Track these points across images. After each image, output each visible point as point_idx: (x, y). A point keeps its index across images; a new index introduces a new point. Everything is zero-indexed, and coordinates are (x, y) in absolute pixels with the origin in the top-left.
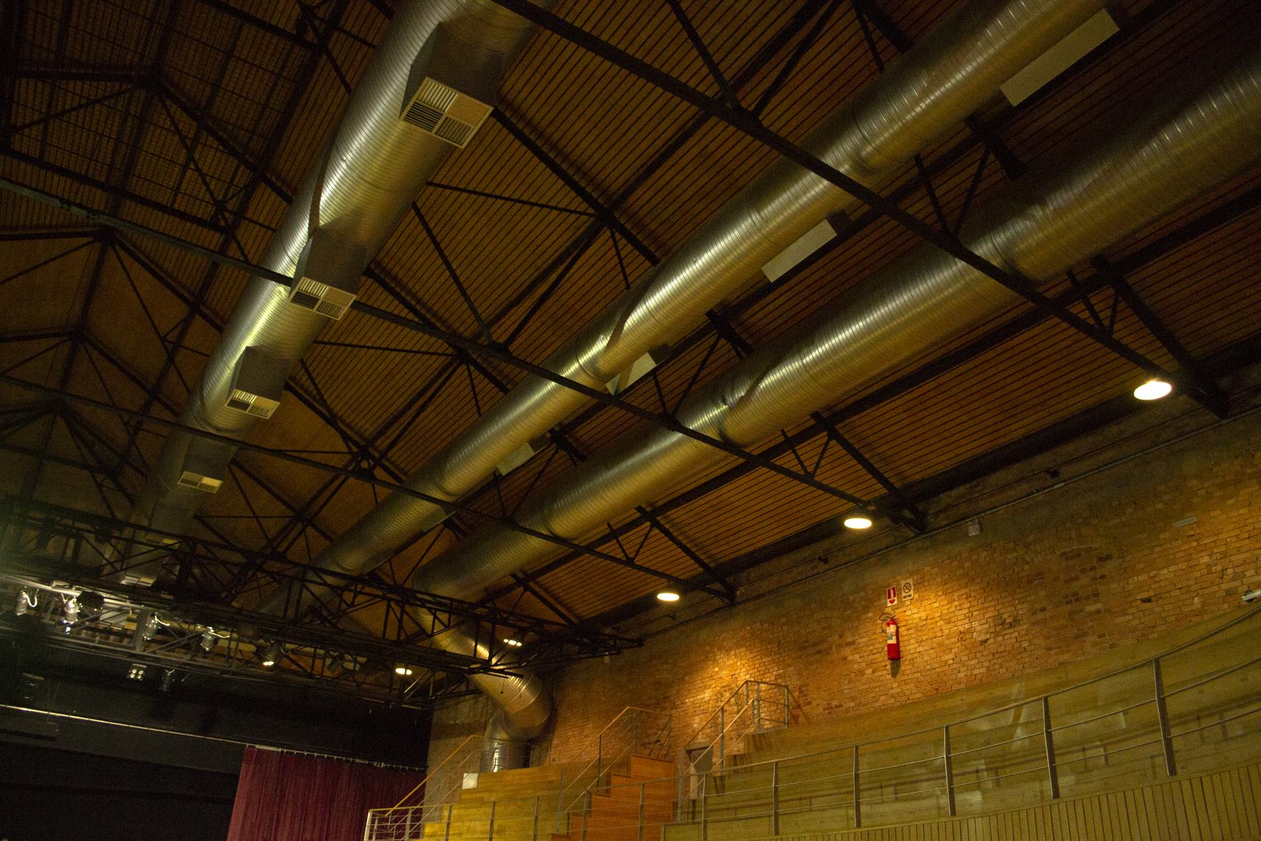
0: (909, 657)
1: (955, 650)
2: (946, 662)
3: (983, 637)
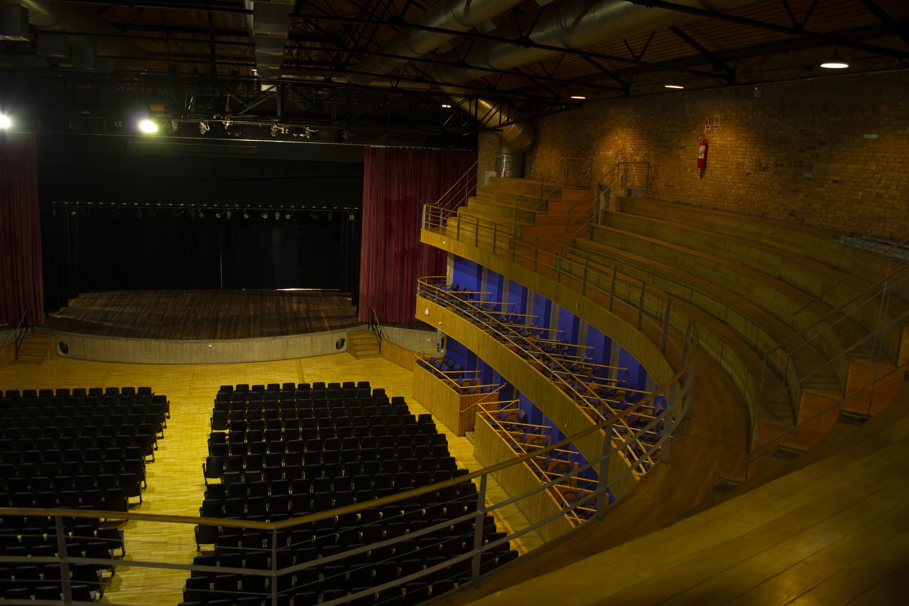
0: (710, 169)
1: (733, 174)
2: (727, 179)
3: (747, 171)
